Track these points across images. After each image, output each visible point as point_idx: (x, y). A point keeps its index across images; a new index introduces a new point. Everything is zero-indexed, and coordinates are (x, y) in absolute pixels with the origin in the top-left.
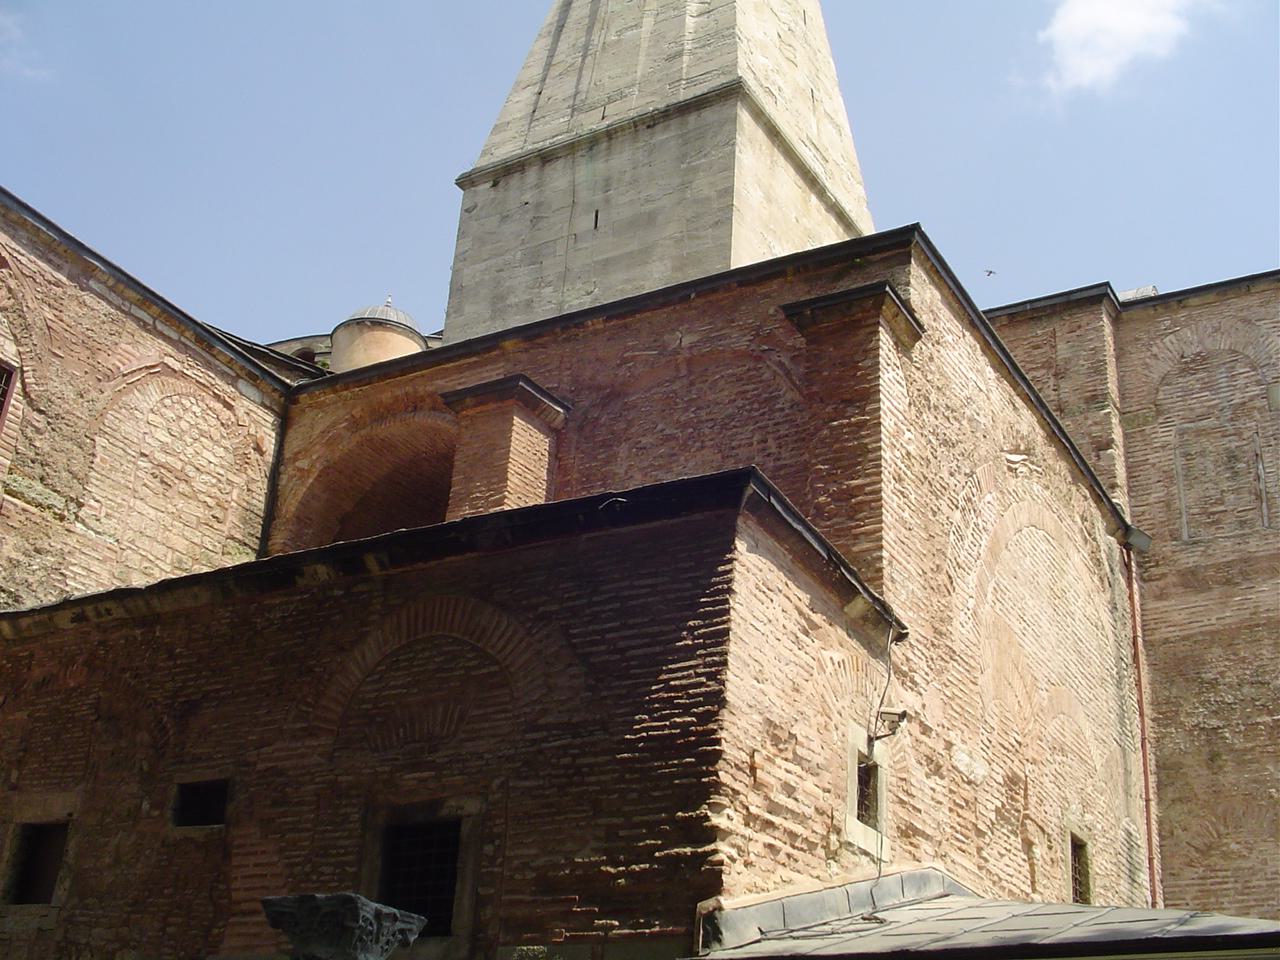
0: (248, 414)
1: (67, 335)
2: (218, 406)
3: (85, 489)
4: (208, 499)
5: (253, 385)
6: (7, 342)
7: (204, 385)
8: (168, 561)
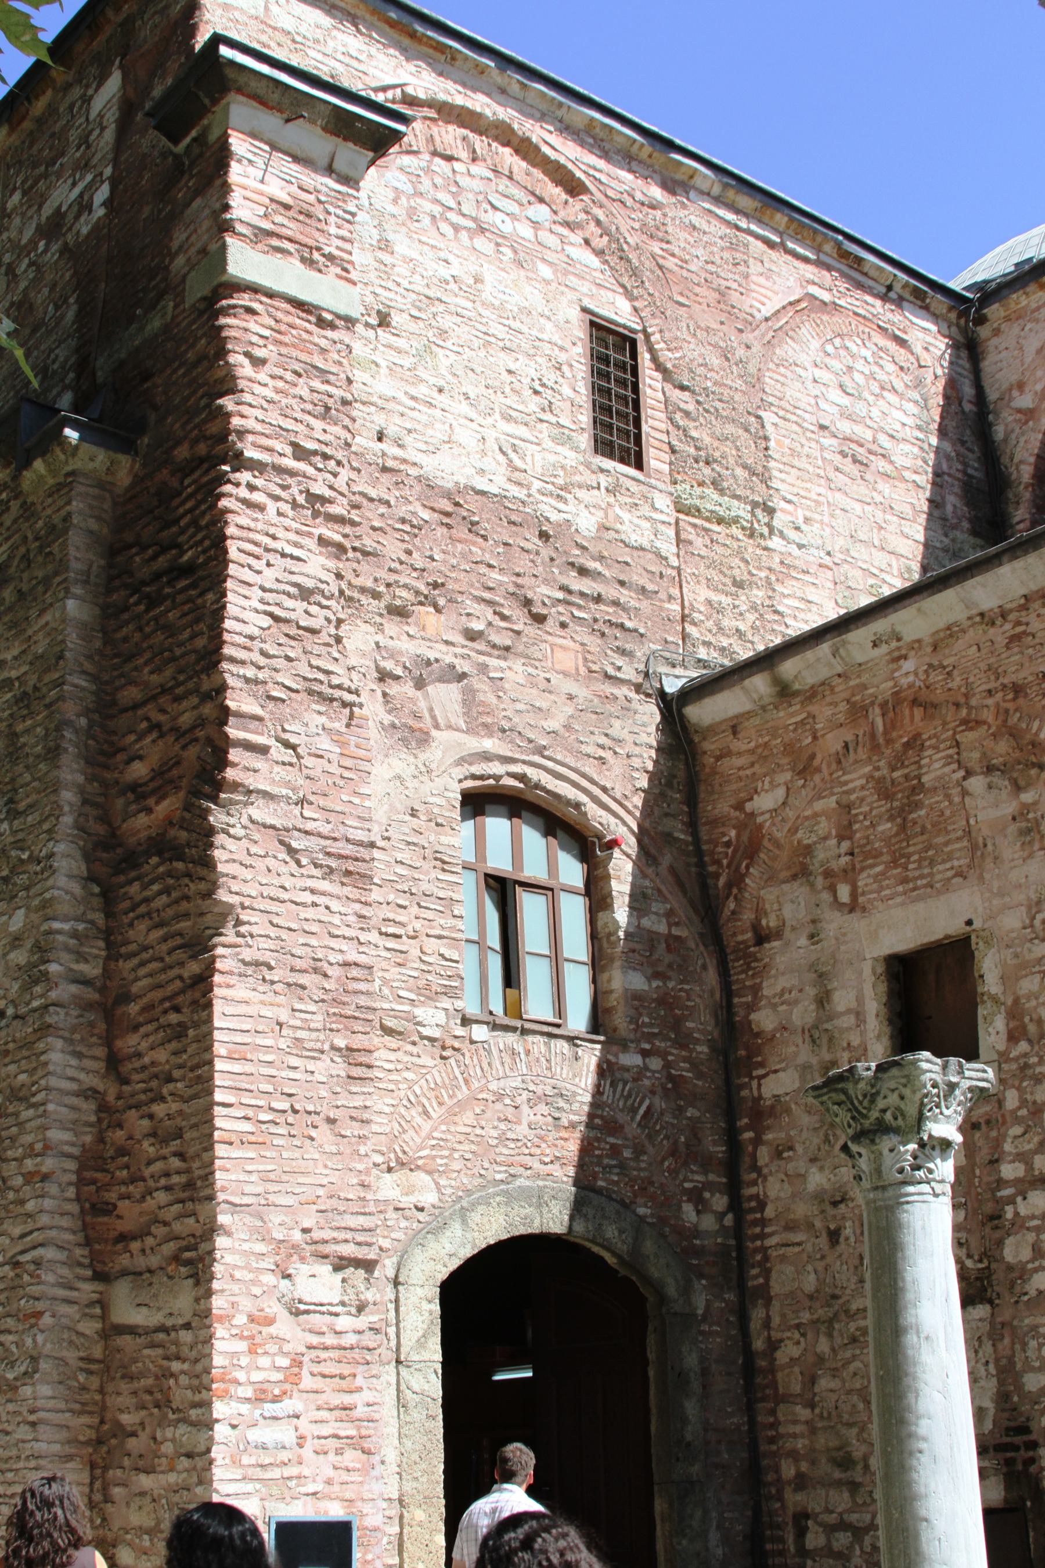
0: (926, 349)
1: (685, 273)
2: (891, 346)
3: (768, 487)
4: (916, 477)
5: (921, 307)
6: (618, 297)
7: (864, 317)
8: (895, 572)
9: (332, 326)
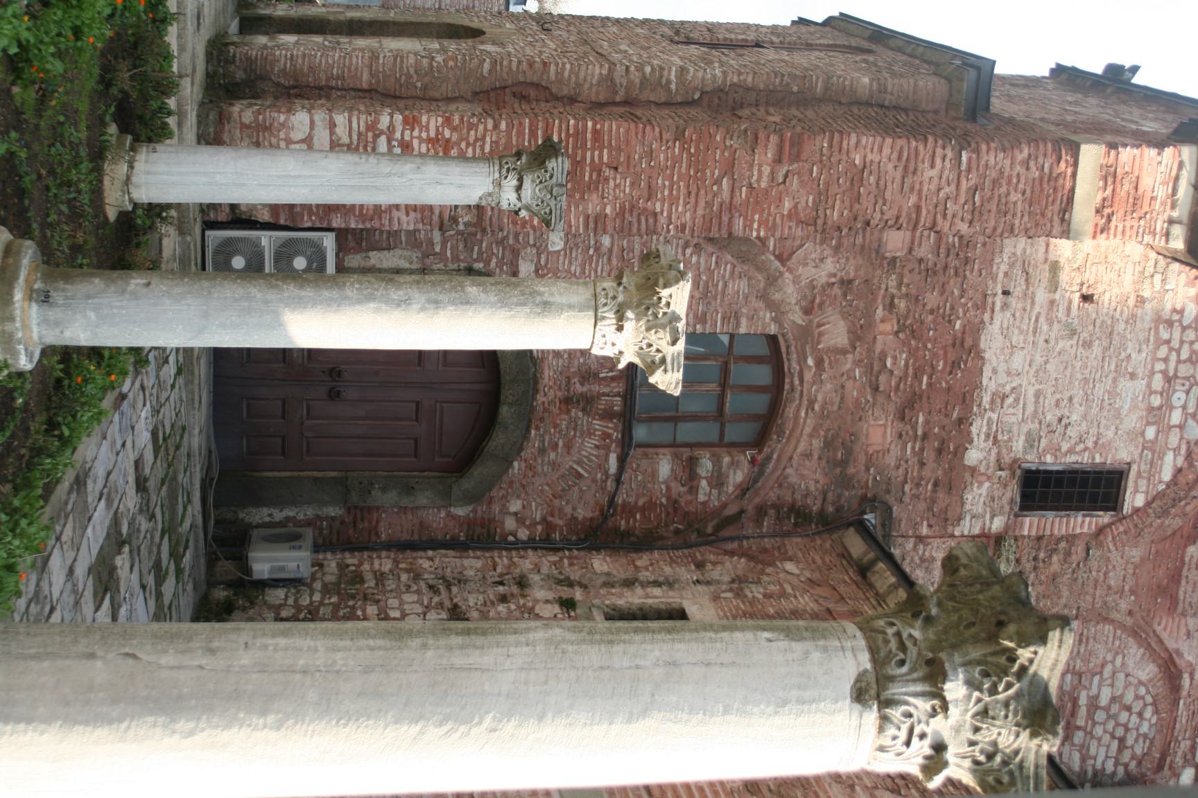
9: (1063, 220)
